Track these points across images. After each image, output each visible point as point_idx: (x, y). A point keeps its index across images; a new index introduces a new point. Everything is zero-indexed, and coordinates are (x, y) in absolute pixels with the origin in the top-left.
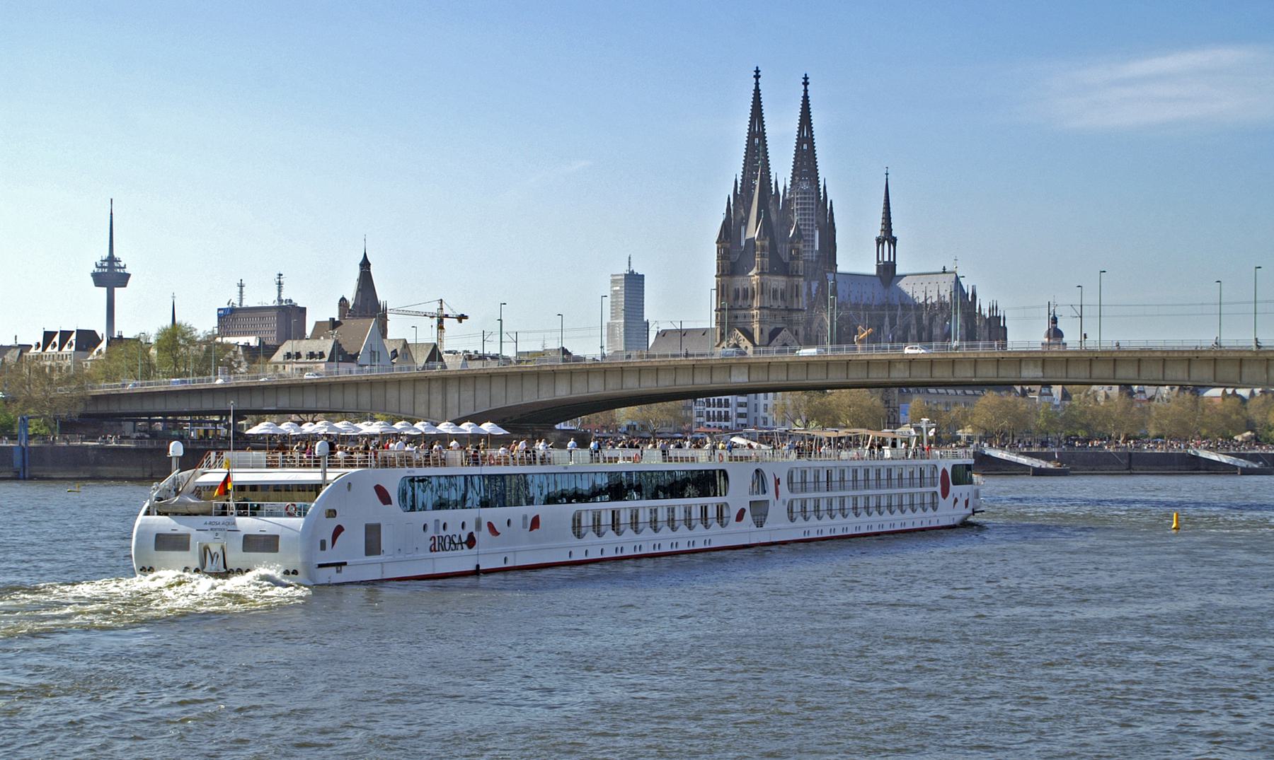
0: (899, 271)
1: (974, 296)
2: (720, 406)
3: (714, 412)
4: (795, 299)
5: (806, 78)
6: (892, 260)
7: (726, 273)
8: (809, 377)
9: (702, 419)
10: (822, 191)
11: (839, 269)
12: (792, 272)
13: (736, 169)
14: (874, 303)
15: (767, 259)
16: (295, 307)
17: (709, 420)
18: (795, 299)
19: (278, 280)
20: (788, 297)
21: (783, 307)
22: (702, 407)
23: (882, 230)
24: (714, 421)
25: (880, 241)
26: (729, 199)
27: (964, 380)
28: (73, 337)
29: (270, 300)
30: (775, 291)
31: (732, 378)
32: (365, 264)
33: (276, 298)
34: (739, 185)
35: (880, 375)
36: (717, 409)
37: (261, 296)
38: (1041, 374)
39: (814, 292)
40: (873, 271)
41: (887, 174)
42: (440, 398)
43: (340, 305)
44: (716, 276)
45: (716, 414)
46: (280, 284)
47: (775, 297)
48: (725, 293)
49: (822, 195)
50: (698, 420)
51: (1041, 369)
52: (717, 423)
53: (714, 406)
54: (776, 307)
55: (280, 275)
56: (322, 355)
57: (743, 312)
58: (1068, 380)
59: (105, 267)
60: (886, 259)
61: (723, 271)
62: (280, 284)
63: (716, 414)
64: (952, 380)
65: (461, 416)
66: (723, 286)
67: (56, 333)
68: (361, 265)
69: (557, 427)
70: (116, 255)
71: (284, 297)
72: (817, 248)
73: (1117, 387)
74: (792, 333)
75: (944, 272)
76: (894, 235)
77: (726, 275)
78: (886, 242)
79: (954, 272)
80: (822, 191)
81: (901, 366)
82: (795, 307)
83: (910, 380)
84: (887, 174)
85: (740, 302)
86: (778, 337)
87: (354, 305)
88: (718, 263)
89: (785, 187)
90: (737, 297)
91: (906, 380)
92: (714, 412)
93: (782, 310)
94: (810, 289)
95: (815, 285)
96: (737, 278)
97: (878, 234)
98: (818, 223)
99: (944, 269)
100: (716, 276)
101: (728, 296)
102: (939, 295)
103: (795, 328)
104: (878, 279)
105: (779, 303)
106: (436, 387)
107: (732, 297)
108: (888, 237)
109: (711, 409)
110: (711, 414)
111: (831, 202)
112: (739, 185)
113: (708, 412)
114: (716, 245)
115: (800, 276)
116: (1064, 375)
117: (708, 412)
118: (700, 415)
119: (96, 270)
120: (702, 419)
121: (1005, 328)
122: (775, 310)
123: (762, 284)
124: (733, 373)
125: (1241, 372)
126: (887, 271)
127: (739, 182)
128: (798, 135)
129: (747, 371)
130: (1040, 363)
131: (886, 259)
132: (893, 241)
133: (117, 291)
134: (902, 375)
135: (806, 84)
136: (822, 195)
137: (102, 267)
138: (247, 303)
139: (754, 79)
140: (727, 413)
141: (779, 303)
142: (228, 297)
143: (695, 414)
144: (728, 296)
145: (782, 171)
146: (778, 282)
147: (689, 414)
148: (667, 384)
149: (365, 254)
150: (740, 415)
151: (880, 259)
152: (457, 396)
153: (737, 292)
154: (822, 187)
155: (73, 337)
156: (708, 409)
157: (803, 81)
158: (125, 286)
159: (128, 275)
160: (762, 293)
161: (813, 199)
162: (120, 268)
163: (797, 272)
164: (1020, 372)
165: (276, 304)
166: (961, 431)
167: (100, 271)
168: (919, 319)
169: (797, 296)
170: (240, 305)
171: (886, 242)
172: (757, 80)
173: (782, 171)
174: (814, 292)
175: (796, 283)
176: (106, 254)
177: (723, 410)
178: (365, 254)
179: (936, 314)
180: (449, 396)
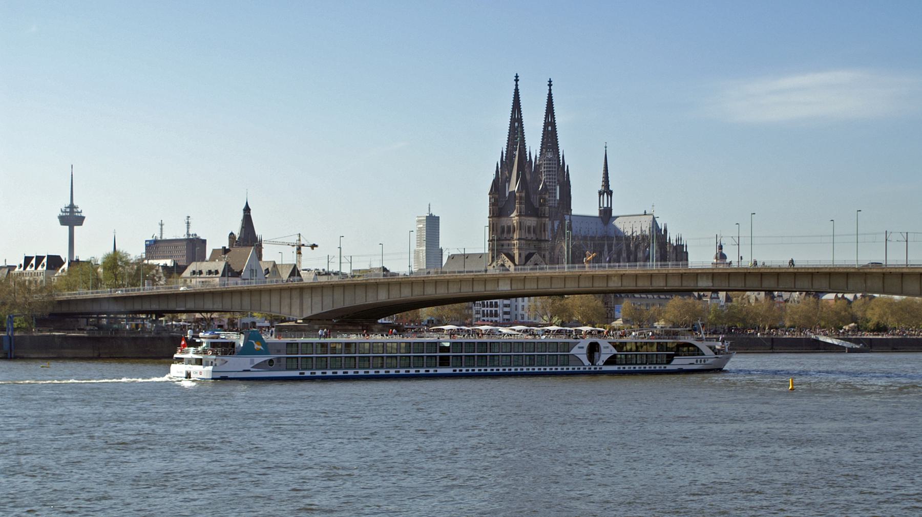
0: (614, 214)
1: (666, 231)
2: (491, 306)
3: (487, 311)
4: (543, 233)
5: (550, 81)
6: (609, 206)
8: (553, 286)
9: (479, 316)
10: (561, 159)
11: (573, 212)
13: (502, 143)
14: (598, 235)
15: (524, 206)
16: (198, 239)
17: (484, 316)
18: (543, 233)
19: (187, 221)
20: (538, 232)
21: (534, 239)
23: (603, 186)
24: (487, 317)
25: (601, 193)
26: (497, 164)
28: (45, 260)
29: (181, 235)
30: (529, 228)
32: (247, 210)
33: (185, 233)
34: (504, 155)
35: (601, 285)
36: (489, 309)
37: (175, 231)
38: (711, 284)
39: (556, 228)
40: (597, 214)
41: (606, 147)
42: (298, 301)
43: (230, 238)
44: (489, 217)
45: (489, 312)
46: (188, 223)
47: (529, 231)
49: (561, 161)
51: (711, 281)
52: (490, 319)
53: (487, 307)
54: (530, 238)
55: (188, 217)
56: (217, 272)
57: (508, 242)
58: (730, 288)
59: (67, 212)
60: (605, 206)
61: (493, 214)
62: (188, 223)
63: (489, 312)
64: (651, 288)
65: (313, 314)
66: (493, 224)
67: (33, 257)
68: (244, 210)
69: (379, 321)
70: (75, 203)
71: (191, 233)
72: (558, 198)
74: (541, 256)
75: (645, 214)
76: (610, 189)
77: (496, 217)
78: (605, 194)
79: (651, 214)
80: (561, 159)
81: (615, 279)
82: (543, 238)
83: (622, 288)
84: (606, 147)
85: (505, 235)
86: (532, 259)
87: (239, 238)
88: (490, 209)
89: (536, 156)
90: (503, 232)
91: (619, 288)
92: (487, 311)
94: (553, 226)
95: (556, 223)
96: (503, 219)
97: (600, 188)
98: (558, 181)
99: (645, 212)
100: (489, 217)
101: (497, 231)
102: (641, 230)
103: (543, 253)
104: (600, 219)
105: (532, 236)
106: (296, 294)
107: (499, 231)
108: (606, 191)
109: (485, 309)
110: (486, 312)
111: (568, 167)
112: (504, 155)
113: (483, 311)
114: (488, 196)
115: (547, 217)
116: (727, 285)
118: (478, 313)
119: (61, 214)
120: (479, 316)
121: (687, 253)
122: (529, 240)
123: (520, 223)
124: (500, 284)
126: (606, 214)
127: (505, 153)
128: (545, 121)
129: (509, 283)
130: (710, 277)
131: (605, 206)
132: (611, 192)
133: (76, 228)
134: (616, 285)
135: (550, 85)
136: (561, 161)
137: (65, 212)
138: (166, 236)
139: (515, 82)
140: (496, 311)
141: (532, 236)
142: (153, 233)
143: (474, 312)
144: (497, 231)
145: (533, 145)
146: (531, 221)
147: (470, 313)
148: (455, 291)
149: (247, 203)
150: (505, 313)
151: (601, 205)
152: (310, 300)
153: (503, 228)
154: (561, 156)
155: (45, 260)
156: (483, 309)
157: (548, 83)
158: (81, 225)
159: (83, 218)
160: (520, 229)
161: (555, 164)
162: (78, 212)
163: (544, 214)
164: (697, 283)
165: (186, 237)
166: (657, 323)
167: (64, 214)
168: (628, 246)
169: (544, 231)
170: (161, 237)
171: (605, 194)
172: (517, 83)
173: (533, 145)
174: (556, 228)
175: (543, 222)
176: (68, 203)
177: (493, 309)
178: (247, 203)
179: (639, 243)
180: (304, 301)
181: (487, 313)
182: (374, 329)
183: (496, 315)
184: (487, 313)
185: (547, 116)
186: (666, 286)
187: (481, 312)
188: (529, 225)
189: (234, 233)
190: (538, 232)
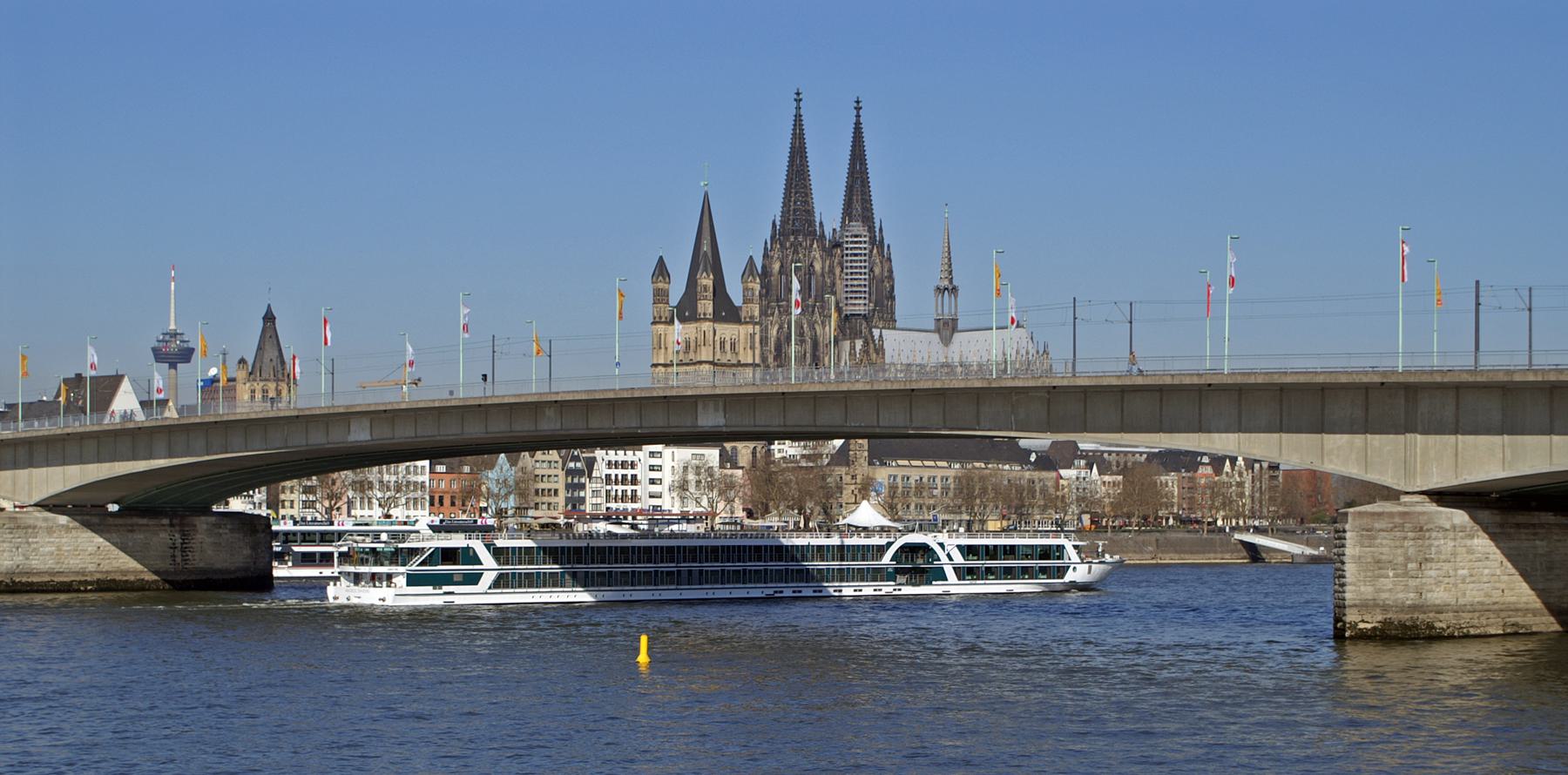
0: (960, 326)
3: (616, 490)
7: (663, 320)
11: (898, 325)
12: (745, 318)
13: (775, 210)
20: (742, 349)
21: (735, 362)
22: (599, 485)
26: (766, 243)
27: (627, 431)
31: (352, 433)
32: (269, 318)
36: (620, 488)
40: (933, 328)
45: (620, 493)
48: (662, 346)
50: (594, 501)
52: (621, 506)
53: (616, 484)
54: (724, 361)
63: (620, 493)
69: (215, 508)
73: (864, 442)
76: (955, 283)
81: (550, 413)
83: (563, 432)
85: (692, 355)
91: (557, 433)
92: (616, 490)
93: (733, 365)
94: (853, 348)
95: (859, 344)
101: (666, 348)
110: (613, 493)
111: (889, 246)
112: (778, 227)
117: (608, 492)
118: (596, 493)
119: (157, 344)
124: (352, 428)
125: (978, 412)
127: (778, 223)
129: (368, 425)
132: (954, 290)
134: (552, 426)
141: (728, 357)
144: (666, 348)
154: (877, 230)
156: (609, 487)
164: (697, 419)
171: (946, 292)
173: (828, 209)
177: (629, 488)
181: (616, 495)
182: (197, 523)
183: (634, 498)
184: (616, 495)
186: (641, 428)
187: (604, 494)
188: (723, 336)
189: (247, 359)
190: (742, 349)
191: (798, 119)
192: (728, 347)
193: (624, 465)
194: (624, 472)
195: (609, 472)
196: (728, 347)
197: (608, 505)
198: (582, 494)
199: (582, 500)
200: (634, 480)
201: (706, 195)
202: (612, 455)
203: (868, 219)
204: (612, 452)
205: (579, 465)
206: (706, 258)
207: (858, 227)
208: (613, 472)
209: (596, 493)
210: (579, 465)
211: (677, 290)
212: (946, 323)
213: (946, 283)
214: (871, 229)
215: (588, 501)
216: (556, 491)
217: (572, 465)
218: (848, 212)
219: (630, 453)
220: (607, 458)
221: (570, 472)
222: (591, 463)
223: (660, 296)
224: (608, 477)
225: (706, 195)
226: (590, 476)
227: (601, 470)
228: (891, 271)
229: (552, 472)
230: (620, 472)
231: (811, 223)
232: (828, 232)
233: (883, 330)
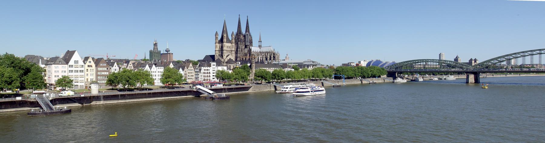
2: (207, 73)
25: (259, 42)
36: (207, 74)
47: (228, 47)
52: (207, 78)
54: (228, 50)
63: (206, 76)
76: (261, 40)
82: (233, 50)
109: (205, 75)
110: (205, 76)
132: (261, 42)
156: (204, 75)
173: (243, 31)
177: (208, 75)
185: (247, 25)
187: (203, 76)
191: (239, 18)
192: (229, 47)
193: (207, 70)
194: (208, 71)
195: (204, 71)
196: (229, 47)
197: (204, 78)
198: (198, 76)
199: (198, 77)
200: (210, 73)
201: (225, 20)
202: (205, 68)
203: (249, 32)
204: (205, 68)
205: (198, 70)
206: (224, 31)
207: (247, 33)
208: (205, 71)
209: (201, 76)
210: (198, 70)
211: (219, 38)
212: (260, 46)
213: (260, 40)
214: (249, 33)
215: (200, 77)
216: (193, 75)
217: (196, 70)
218: (246, 32)
219: (209, 67)
220: (204, 69)
221: (196, 72)
222: (200, 70)
223: (216, 38)
224: (204, 72)
225: (225, 20)
226: (200, 72)
227: (202, 71)
228: (252, 39)
229: (192, 72)
230: (207, 71)
231: (241, 32)
232: (243, 34)
233: (252, 47)
